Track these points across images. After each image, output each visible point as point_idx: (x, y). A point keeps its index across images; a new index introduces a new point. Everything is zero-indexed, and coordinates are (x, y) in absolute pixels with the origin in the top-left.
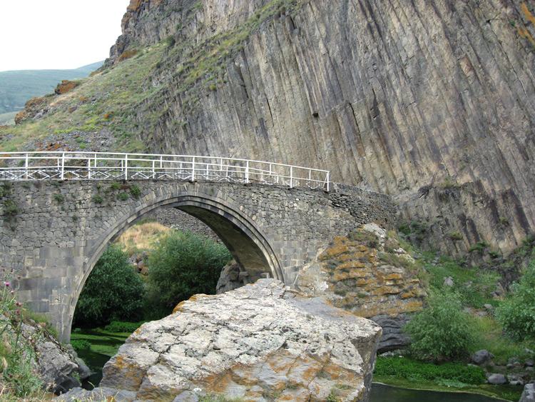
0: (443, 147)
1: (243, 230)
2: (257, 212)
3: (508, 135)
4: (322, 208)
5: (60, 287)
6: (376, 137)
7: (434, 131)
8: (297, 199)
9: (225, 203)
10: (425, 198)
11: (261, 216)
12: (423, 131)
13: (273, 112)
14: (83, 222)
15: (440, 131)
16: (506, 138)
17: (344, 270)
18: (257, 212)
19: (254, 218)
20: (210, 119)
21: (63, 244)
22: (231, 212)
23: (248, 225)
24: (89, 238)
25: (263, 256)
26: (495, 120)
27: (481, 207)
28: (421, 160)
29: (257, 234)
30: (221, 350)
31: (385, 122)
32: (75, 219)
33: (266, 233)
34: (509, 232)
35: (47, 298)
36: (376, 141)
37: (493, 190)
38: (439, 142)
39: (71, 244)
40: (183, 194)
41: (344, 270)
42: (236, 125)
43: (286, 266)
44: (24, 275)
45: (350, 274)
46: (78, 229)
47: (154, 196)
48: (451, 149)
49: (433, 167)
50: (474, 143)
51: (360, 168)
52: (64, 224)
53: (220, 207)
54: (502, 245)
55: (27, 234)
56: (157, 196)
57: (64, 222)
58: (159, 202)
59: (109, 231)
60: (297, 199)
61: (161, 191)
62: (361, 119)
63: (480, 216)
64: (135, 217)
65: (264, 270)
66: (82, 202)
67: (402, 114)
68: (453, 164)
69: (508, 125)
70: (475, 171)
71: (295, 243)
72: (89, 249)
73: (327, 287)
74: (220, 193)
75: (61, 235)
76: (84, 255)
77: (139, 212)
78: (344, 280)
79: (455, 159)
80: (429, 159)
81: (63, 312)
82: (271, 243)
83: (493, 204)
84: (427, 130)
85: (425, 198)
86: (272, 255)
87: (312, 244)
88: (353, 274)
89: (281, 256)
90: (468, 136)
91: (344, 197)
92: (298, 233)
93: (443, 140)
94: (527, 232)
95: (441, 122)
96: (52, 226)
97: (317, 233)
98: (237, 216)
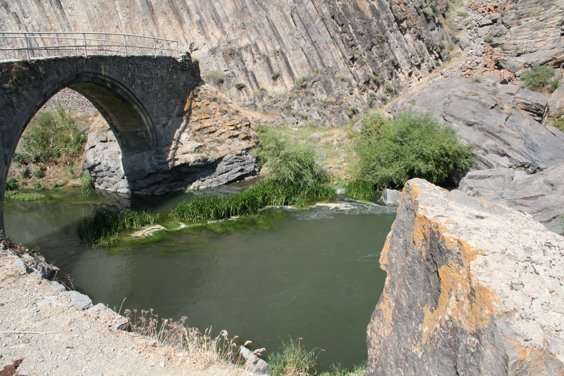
1: (126, 98)
3: (277, 9)
8: (160, 67)
9: (112, 76)
10: (214, 56)
16: (276, 11)
18: (134, 81)
19: (133, 87)
22: (116, 83)
23: (129, 94)
25: (140, 118)
27: (259, 63)
28: (206, 27)
29: (136, 101)
30: (556, 292)
33: (143, 99)
34: (281, 80)
37: (266, 49)
38: (220, 13)
40: (80, 70)
43: (158, 125)
47: (57, 76)
48: (231, 19)
49: (218, 33)
50: (250, 14)
51: (155, 33)
53: (108, 80)
54: (276, 89)
56: (59, 75)
60: (160, 67)
61: (61, 69)
63: (259, 69)
65: (139, 130)
68: (233, 30)
77: (45, 94)
78: (199, 130)
79: (234, 26)
82: (146, 107)
83: (268, 61)
85: (214, 56)
86: (148, 117)
88: (206, 123)
89: (154, 116)
90: (245, 9)
93: (224, 12)
98: (121, 86)
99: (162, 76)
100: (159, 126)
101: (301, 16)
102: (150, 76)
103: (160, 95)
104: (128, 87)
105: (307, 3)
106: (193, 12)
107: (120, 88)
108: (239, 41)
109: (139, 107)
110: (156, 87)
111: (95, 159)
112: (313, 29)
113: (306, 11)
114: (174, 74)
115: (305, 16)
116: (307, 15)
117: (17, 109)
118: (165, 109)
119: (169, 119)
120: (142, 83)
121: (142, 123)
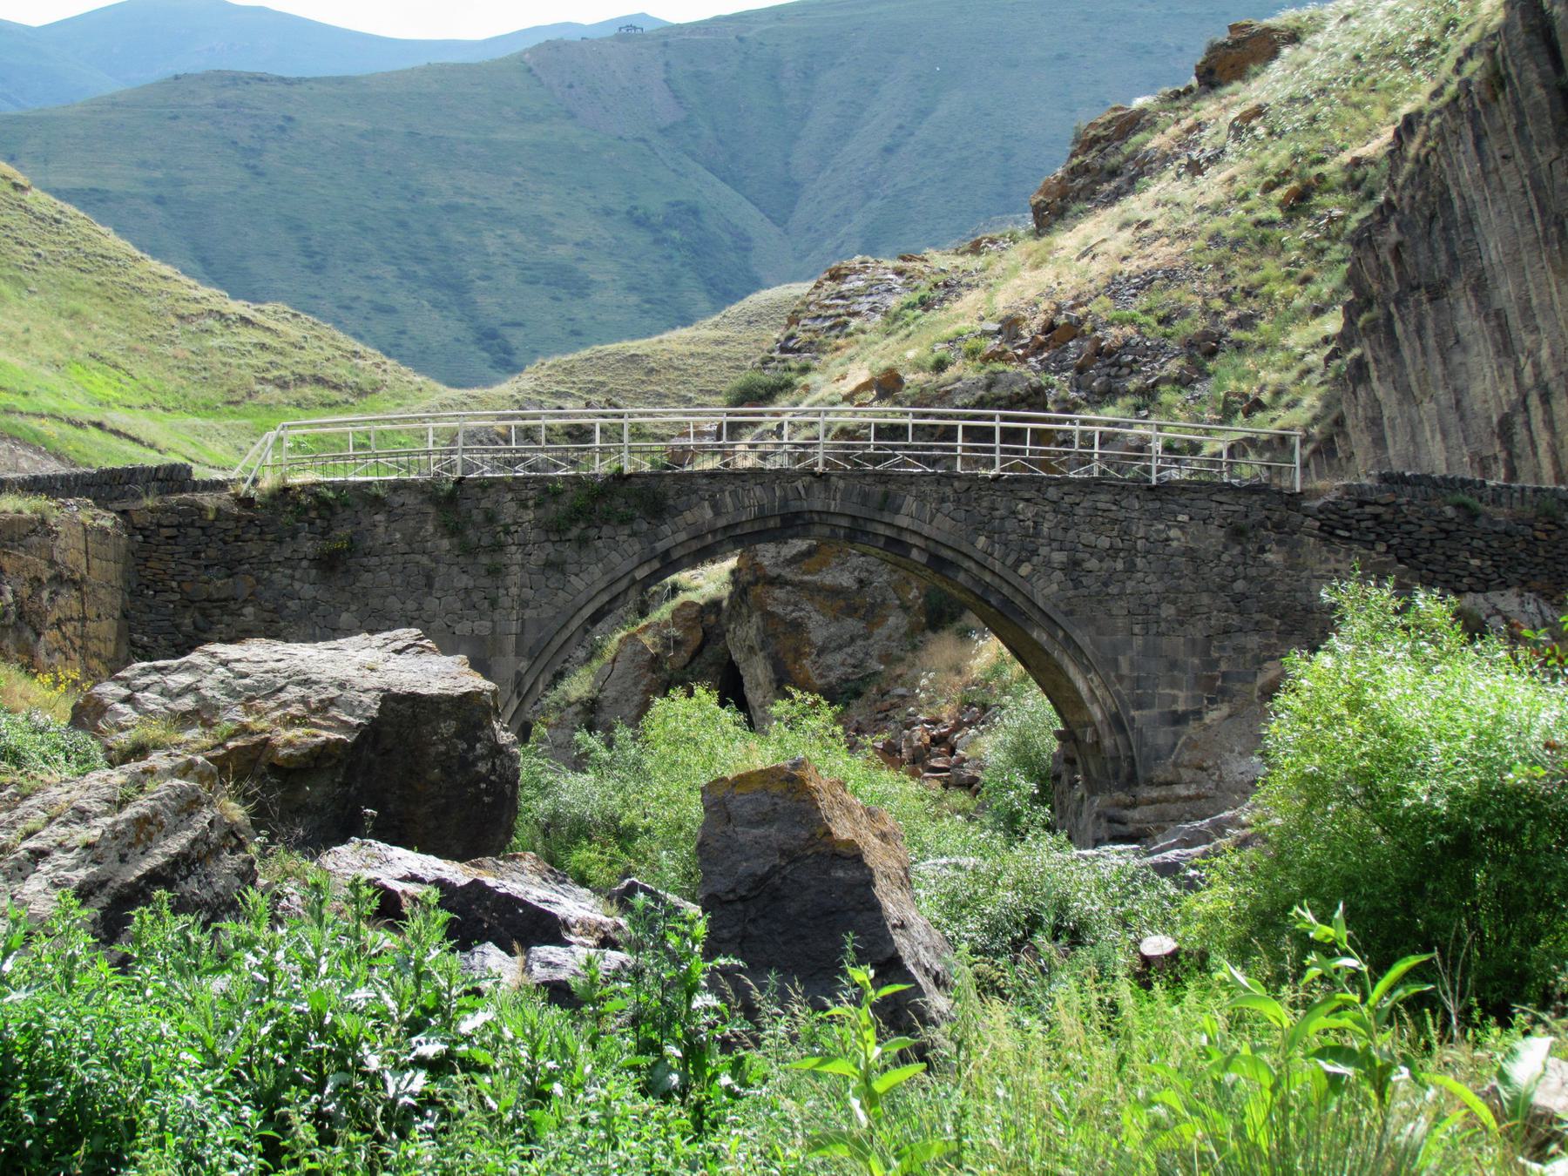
2: (1035, 552)
4: (1279, 543)
8: (1182, 518)
11: (1047, 563)
14: (515, 576)
18: (1035, 552)
19: (1025, 570)
20: (1470, 221)
24: (528, 613)
32: (495, 572)
39: (483, 627)
40: (795, 506)
46: (502, 591)
52: (465, 581)
55: (375, 602)
57: (465, 577)
58: (726, 528)
59: (582, 598)
61: (728, 500)
64: (656, 565)
66: (512, 529)
71: (1175, 644)
72: (530, 639)
74: (910, 504)
75: (458, 605)
76: (517, 654)
77: (667, 553)
82: (1082, 638)
87: (1241, 650)
91: (1368, 509)
92: (1188, 614)
96: (437, 585)
97: (1257, 617)
98: (967, 564)
100: (1145, 712)
117: (573, 578)
119: (1211, 701)
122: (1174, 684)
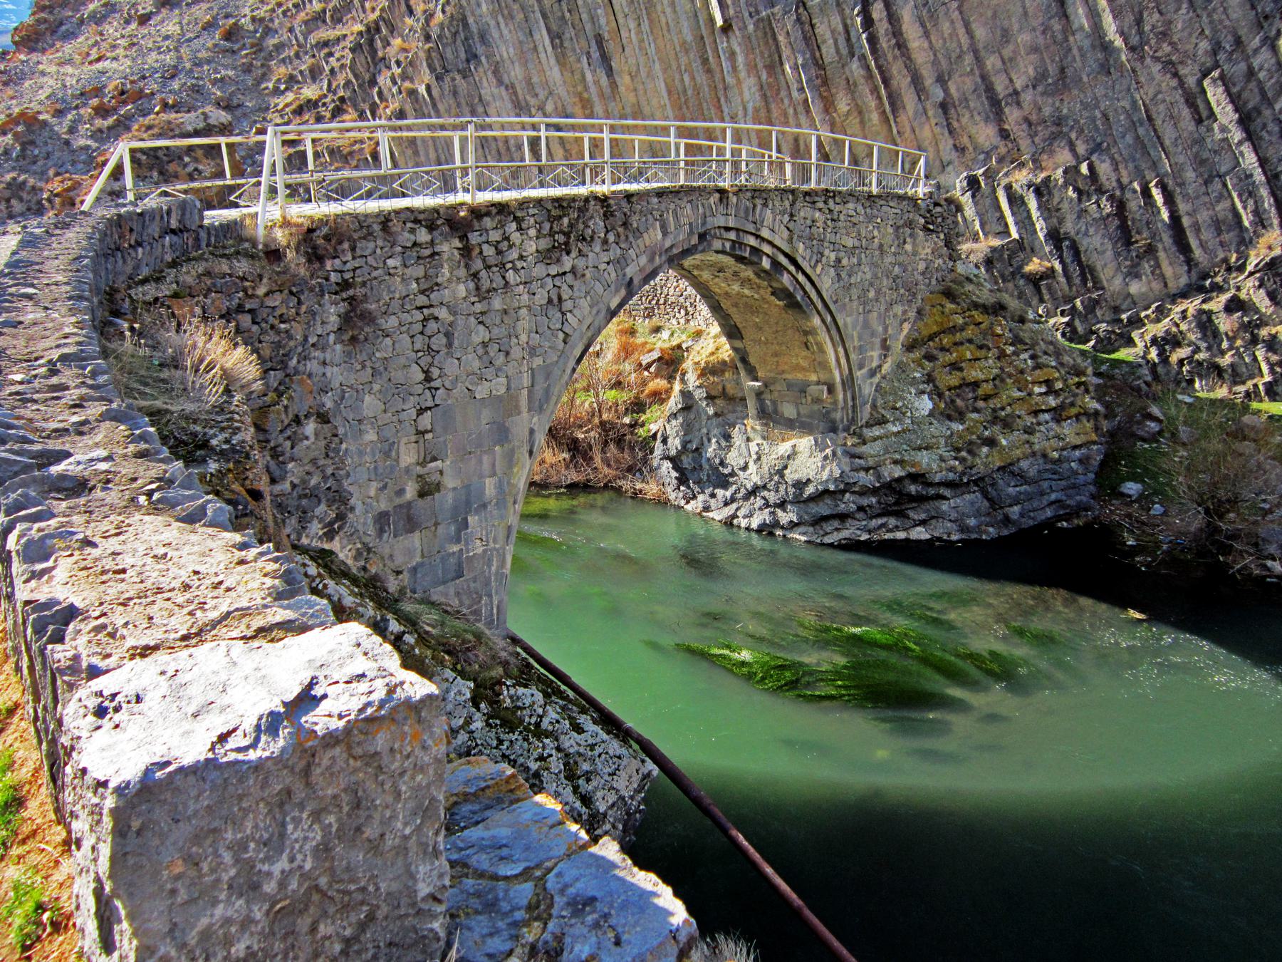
0: (1010, 95)
1: (799, 298)
5: (484, 506)
6: (862, 72)
7: (992, 62)
9: (778, 242)
10: (973, 196)
12: (969, 59)
13: (621, 21)
14: (525, 321)
15: (1004, 63)
16: (1158, 77)
17: (955, 366)
18: (822, 255)
19: (819, 269)
20: (483, 37)
21: (482, 391)
22: (783, 260)
23: (808, 287)
24: (538, 361)
26: (1137, 38)
31: (885, 43)
33: (835, 302)
35: (458, 541)
36: (862, 81)
37: (1119, 181)
41: (955, 366)
42: (540, 49)
44: (401, 492)
45: (965, 373)
46: (514, 340)
47: (660, 236)
48: (1027, 97)
53: (767, 249)
56: (665, 233)
62: (828, 35)
63: (1092, 231)
66: (519, 264)
67: (923, 25)
69: (1167, 48)
70: (1079, 143)
73: (930, 405)
75: (476, 364)
76: (530, 410)
77: (631, 279)
79: (1034, 118)
80: (977, 118)
81: (493, 569)
84: (978, 60)
86: (841, 350)
93: (1011, 80)
94: (1190, 262)
95: (1008, 42)
98: (792, 268)
99: (881, 246)
101: (1235, 90)
102: (857, 244)
103: (872, 294)
104: (808, 270)
105: (1256, 51)
106: (929, 81)
107: (789, 272)
108: (1045, 157)
109: (823, 321)
110: (866, 273)
111: (688, 438)
112: (1264, 126)
113: (1251, 73)
114: (908, 240)
115: (1243, 89)
116: (1253, 85)
118: (880, 329)
120: (838, 260)
121: (824, 365)
122: (872, 350)
